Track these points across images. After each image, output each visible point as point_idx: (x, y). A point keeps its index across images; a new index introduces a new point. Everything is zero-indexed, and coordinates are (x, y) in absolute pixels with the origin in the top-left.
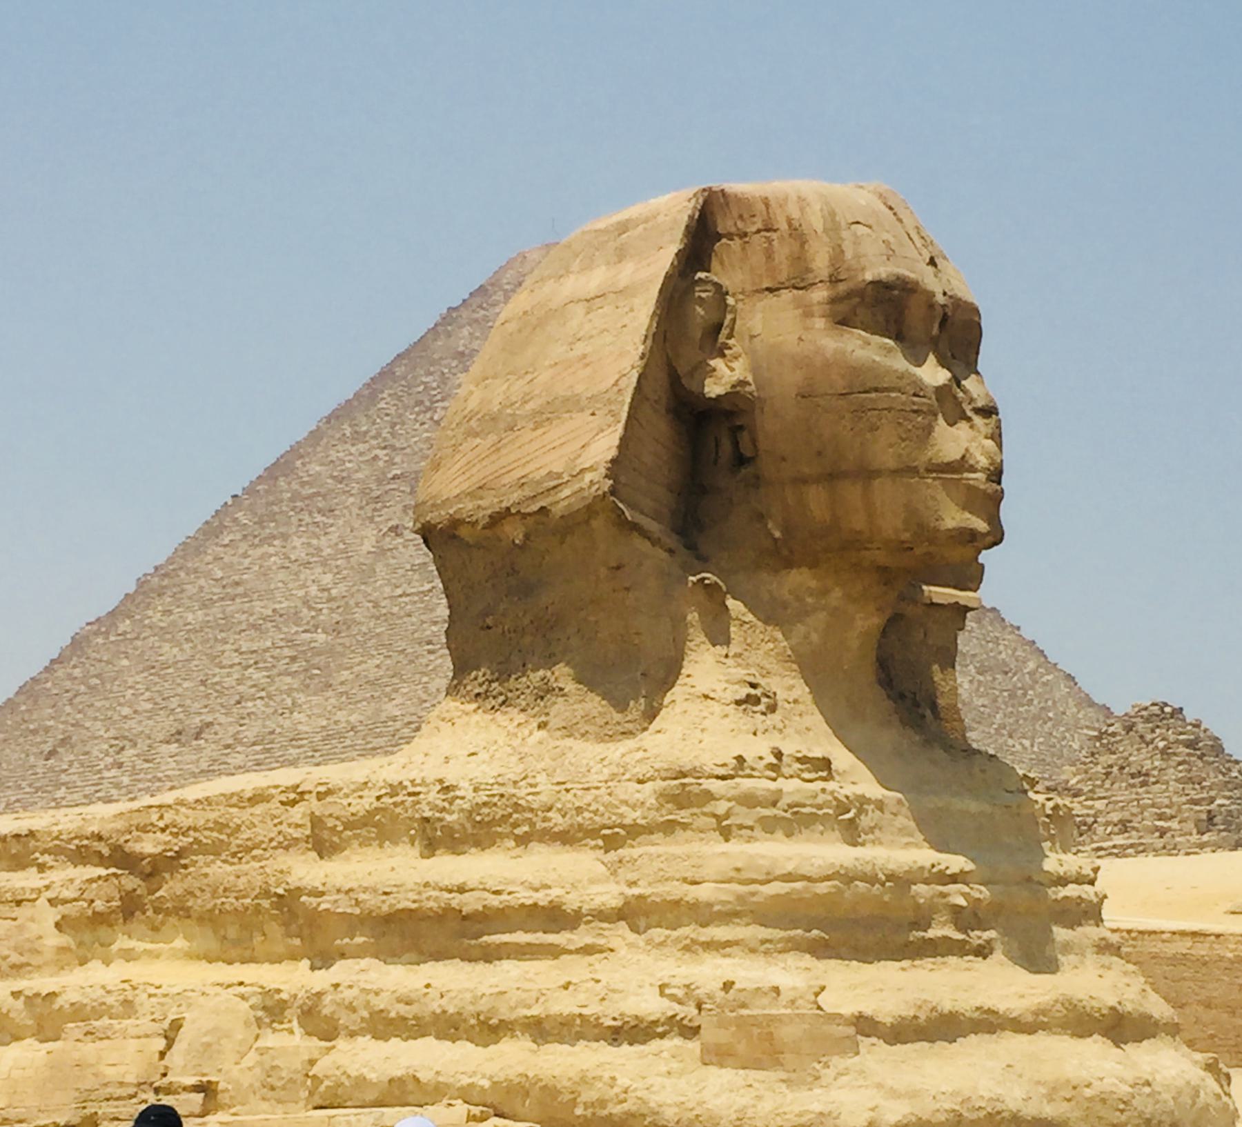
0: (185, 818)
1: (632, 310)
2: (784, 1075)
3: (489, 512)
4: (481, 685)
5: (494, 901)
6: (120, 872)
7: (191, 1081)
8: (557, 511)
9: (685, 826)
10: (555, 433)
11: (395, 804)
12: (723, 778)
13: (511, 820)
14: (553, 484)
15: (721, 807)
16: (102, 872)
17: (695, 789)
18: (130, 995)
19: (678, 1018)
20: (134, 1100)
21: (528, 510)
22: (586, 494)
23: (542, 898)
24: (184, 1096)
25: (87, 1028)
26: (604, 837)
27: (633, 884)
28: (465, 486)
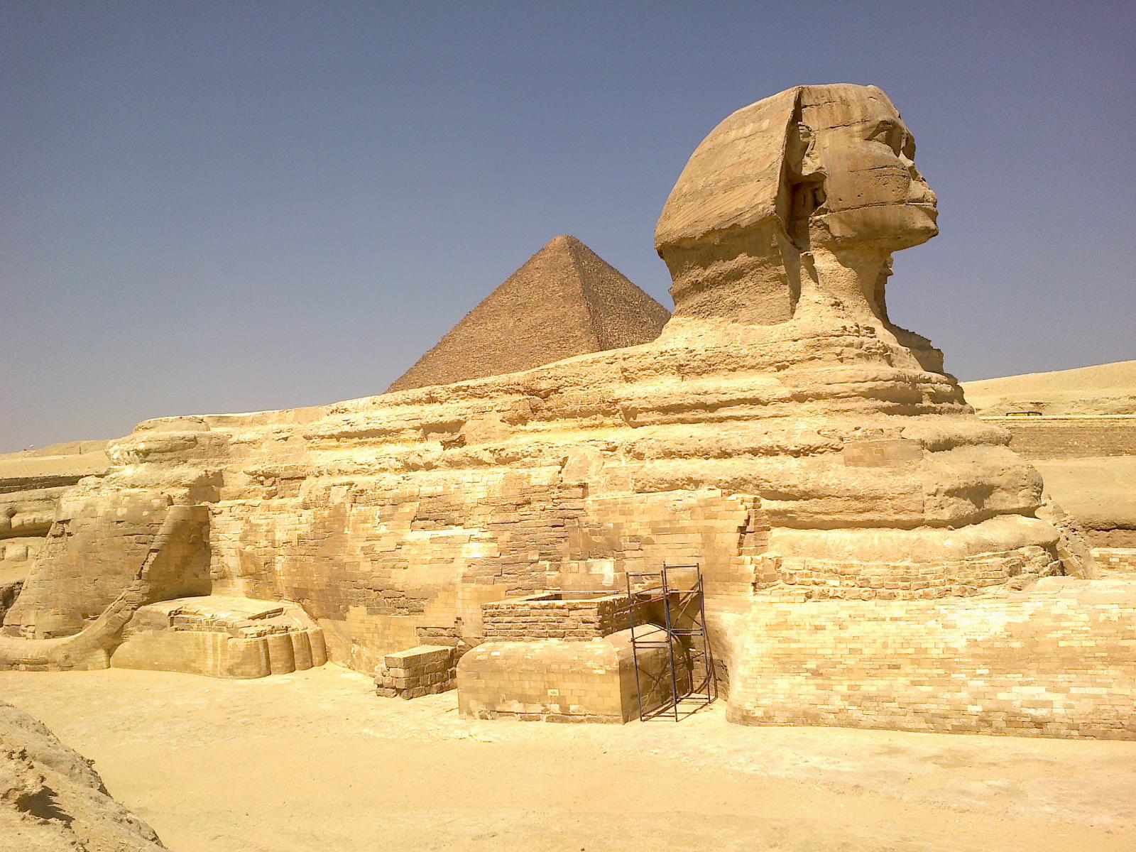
0: (559, 373)
1: (772, 137)
2: (890, 470)
3: (702, 231)
4: (696, 309)
5: (725, 398)
6: (529, 397)
7: (577, 483)
8: (743, 225)
9: (820, 359)
10: (736, 193)
11: (664, 360)
12: (838, 336)
13: (725, 362)
14: (739, 213)
15: (838, 350)
16: (522, 398)
17: (824, 342)
18: (540, 447)
19: (830, 445)
20: (548, 492)
21: (724, 227)
22: (761, 214)
23: (749, 395)
24: (574, 490)
25: (522, 463)
26: (777, 367)
27: (796, 386)
28: (686, 223)
